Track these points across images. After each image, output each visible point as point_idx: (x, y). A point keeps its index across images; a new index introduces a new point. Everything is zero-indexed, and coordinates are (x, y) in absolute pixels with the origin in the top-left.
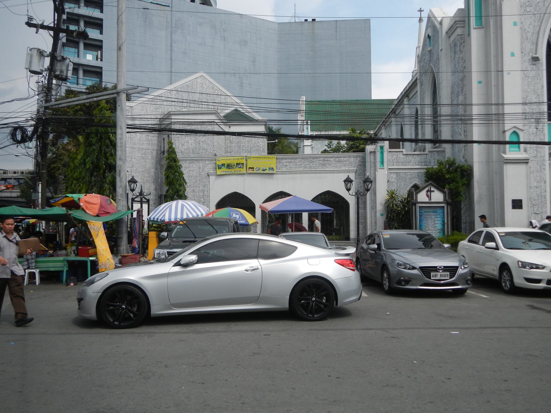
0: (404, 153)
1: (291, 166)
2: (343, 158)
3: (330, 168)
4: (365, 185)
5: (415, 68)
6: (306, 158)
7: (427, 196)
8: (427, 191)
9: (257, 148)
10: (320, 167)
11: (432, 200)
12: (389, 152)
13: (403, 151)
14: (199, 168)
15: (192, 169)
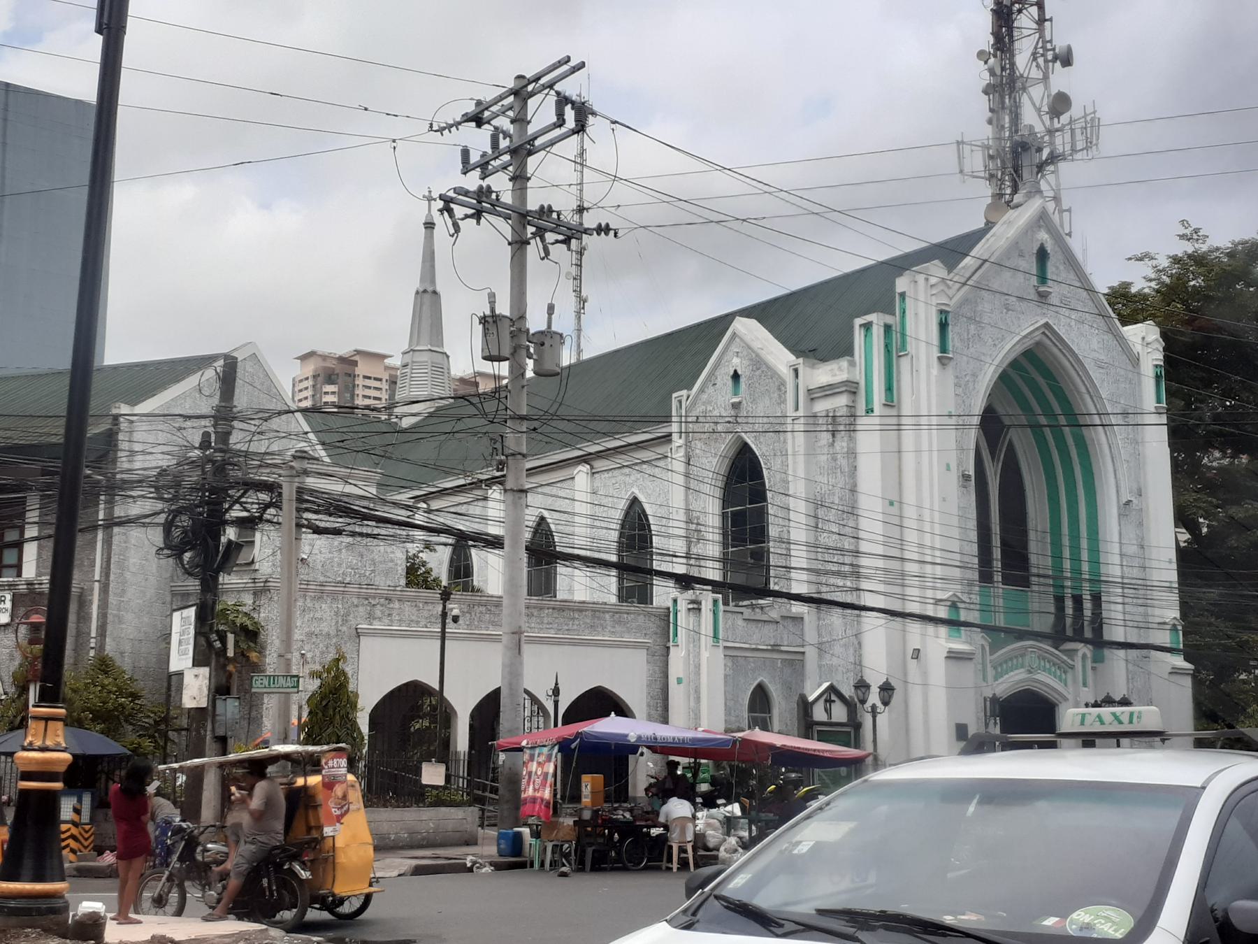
0: (746, 616)
1: (533, 625)
2: (625, 616)
3: (603, 635)
4: (859, 692)
5: (410, 345)
6: (561, 609)
7: (826, 710)
8: (826, 701)
9: (391, 564)
10: (587, 631)
11: (834, 720)
12: (689, 609)
13: (742, 613)
14: (337, 614)
15: (318, 615)
